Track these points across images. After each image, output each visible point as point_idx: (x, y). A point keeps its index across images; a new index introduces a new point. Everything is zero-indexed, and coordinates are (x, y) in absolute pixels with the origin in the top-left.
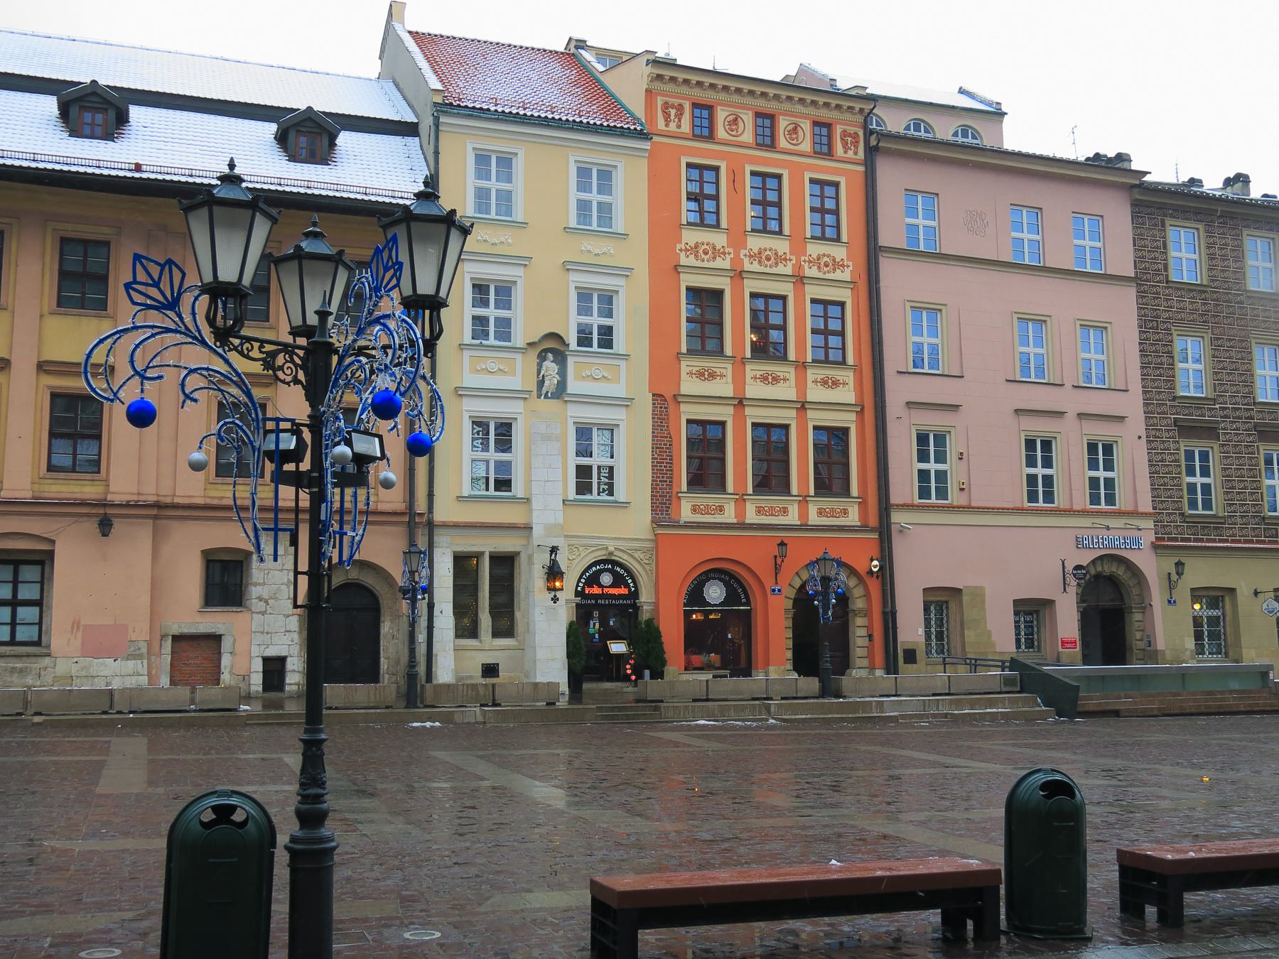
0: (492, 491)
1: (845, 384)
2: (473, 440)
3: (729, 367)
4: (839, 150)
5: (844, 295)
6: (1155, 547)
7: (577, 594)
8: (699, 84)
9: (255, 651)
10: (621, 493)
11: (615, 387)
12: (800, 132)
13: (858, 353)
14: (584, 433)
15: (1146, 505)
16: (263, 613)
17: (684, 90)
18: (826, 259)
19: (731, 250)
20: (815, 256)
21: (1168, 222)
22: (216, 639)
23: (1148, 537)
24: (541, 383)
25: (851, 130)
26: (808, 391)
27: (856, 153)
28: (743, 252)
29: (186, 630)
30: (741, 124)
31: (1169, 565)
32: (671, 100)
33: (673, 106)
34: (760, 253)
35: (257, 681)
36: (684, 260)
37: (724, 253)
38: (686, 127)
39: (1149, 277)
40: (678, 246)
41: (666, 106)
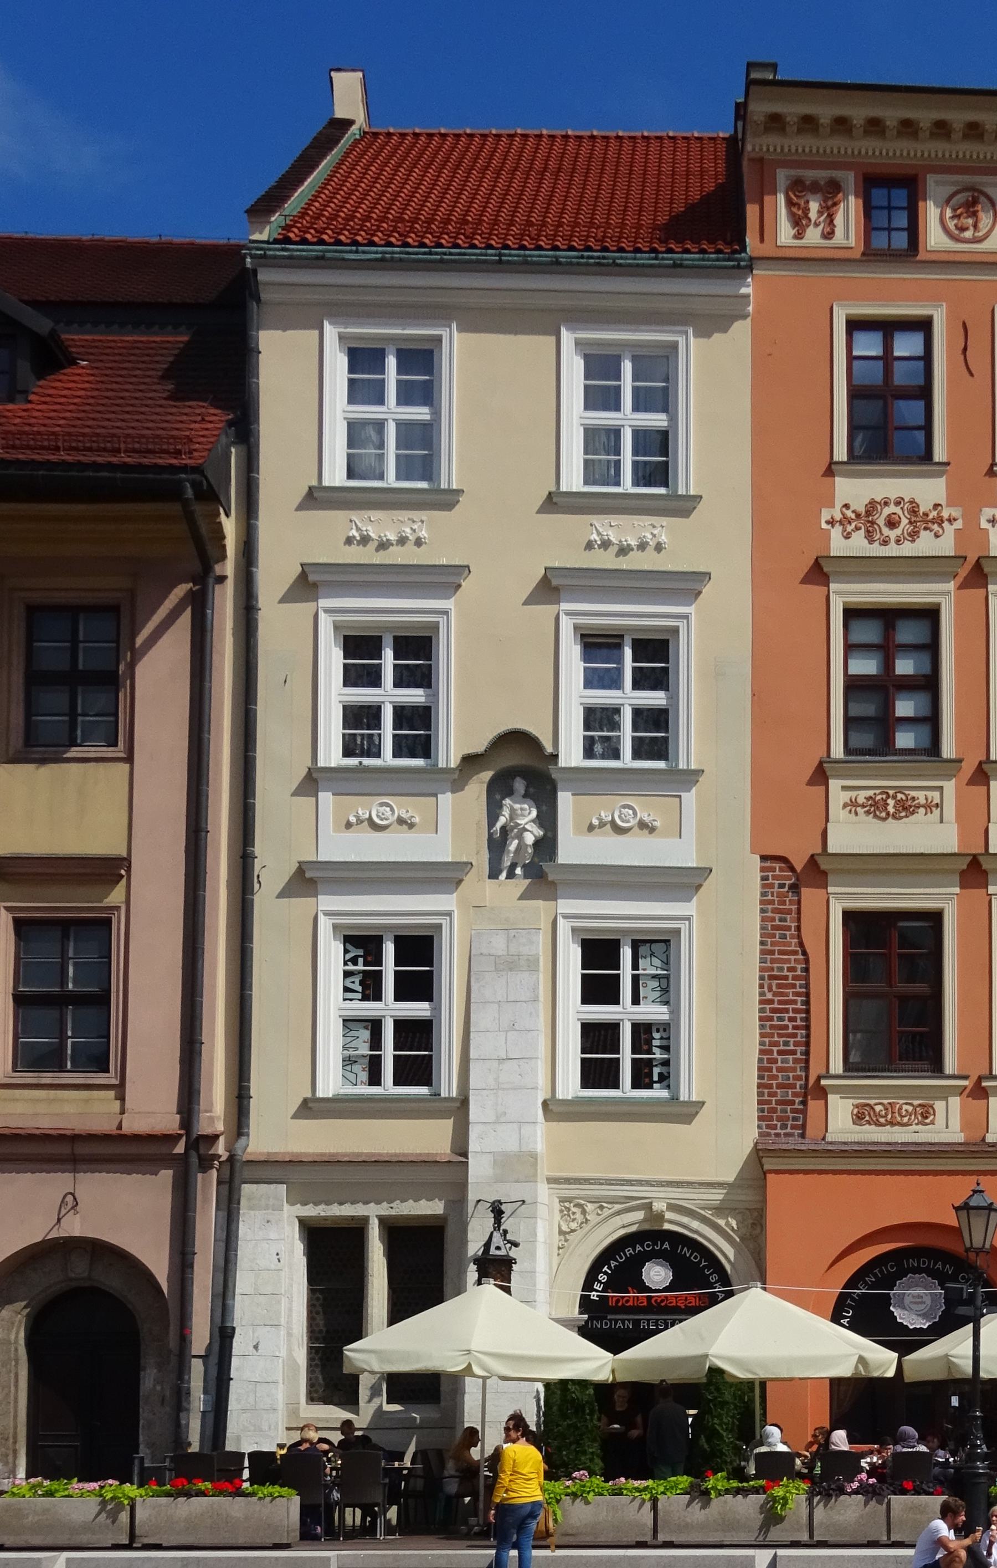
0: (388, 1086)
2: (347, 974)
7: (585, 1304)
10: (693, 1079)
11: (689, 841)
14: (599, 951)
19: (955, 512)
24: (497, 845)
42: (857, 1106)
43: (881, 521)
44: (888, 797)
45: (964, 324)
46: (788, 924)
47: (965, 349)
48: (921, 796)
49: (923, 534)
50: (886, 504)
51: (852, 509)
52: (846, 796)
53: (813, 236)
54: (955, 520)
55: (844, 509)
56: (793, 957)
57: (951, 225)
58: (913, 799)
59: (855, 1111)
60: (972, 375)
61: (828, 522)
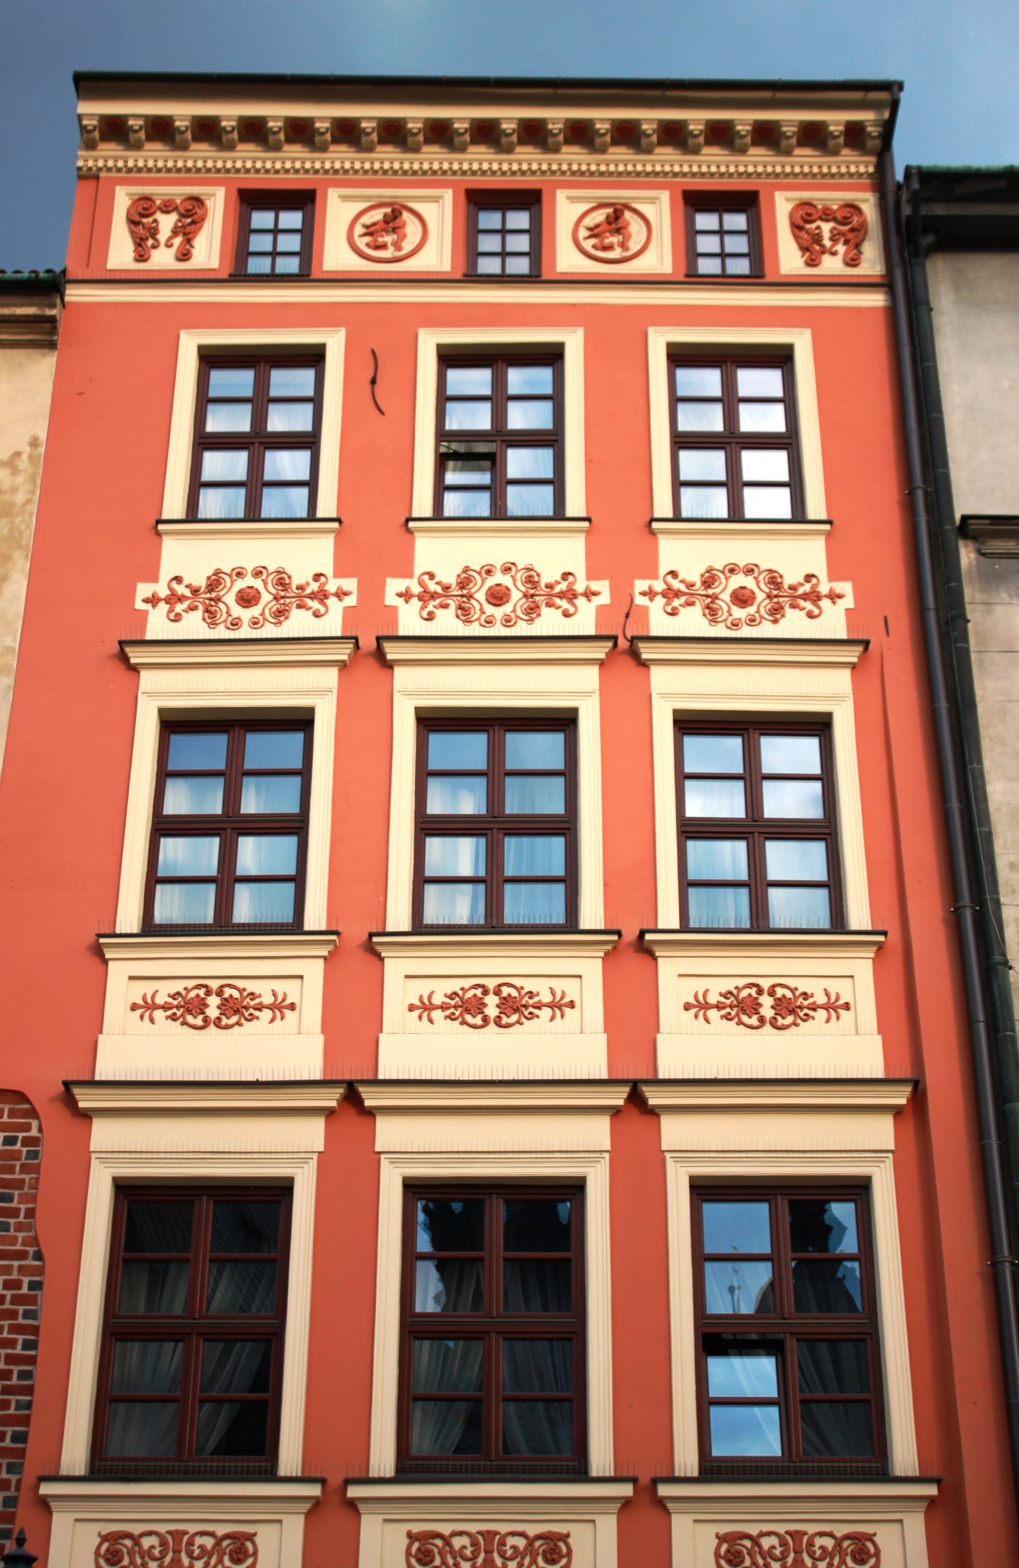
1: (834, 1007)
3: (314, 971)
4: (789, 258)
5: (826, 688)
12: (635, 228)
17: (202, 154)
18: (738, 581)
19: (350, 584)
20: (693, 574)
25: (833, 198)
26: (664, 1043)
27: (852, 262)
28: (394, 586)
30: (412, 229)
32: (161, 192)
33: (167, 208)
34: (464, 582)
37: (321, 596)
38: (209, 249)
40: (144, 590)
42: (104, 1538)
43: (230, 598)
44: (208, 993)
45: (373, 352)
46: (15, 1204)
47: (373, 382)
48: (265, 991)
49: (295, 613)
50: (239, 575)
51: (186, 582)
52: (138, 991)
53: (163, 259)
54: (346, 594)
55: (174, 584)
56: (16, 1264)
57: (362, 243)
58: (252, 995)
59: (105, 1546)
60: (382, 412)
61: (146, 601)
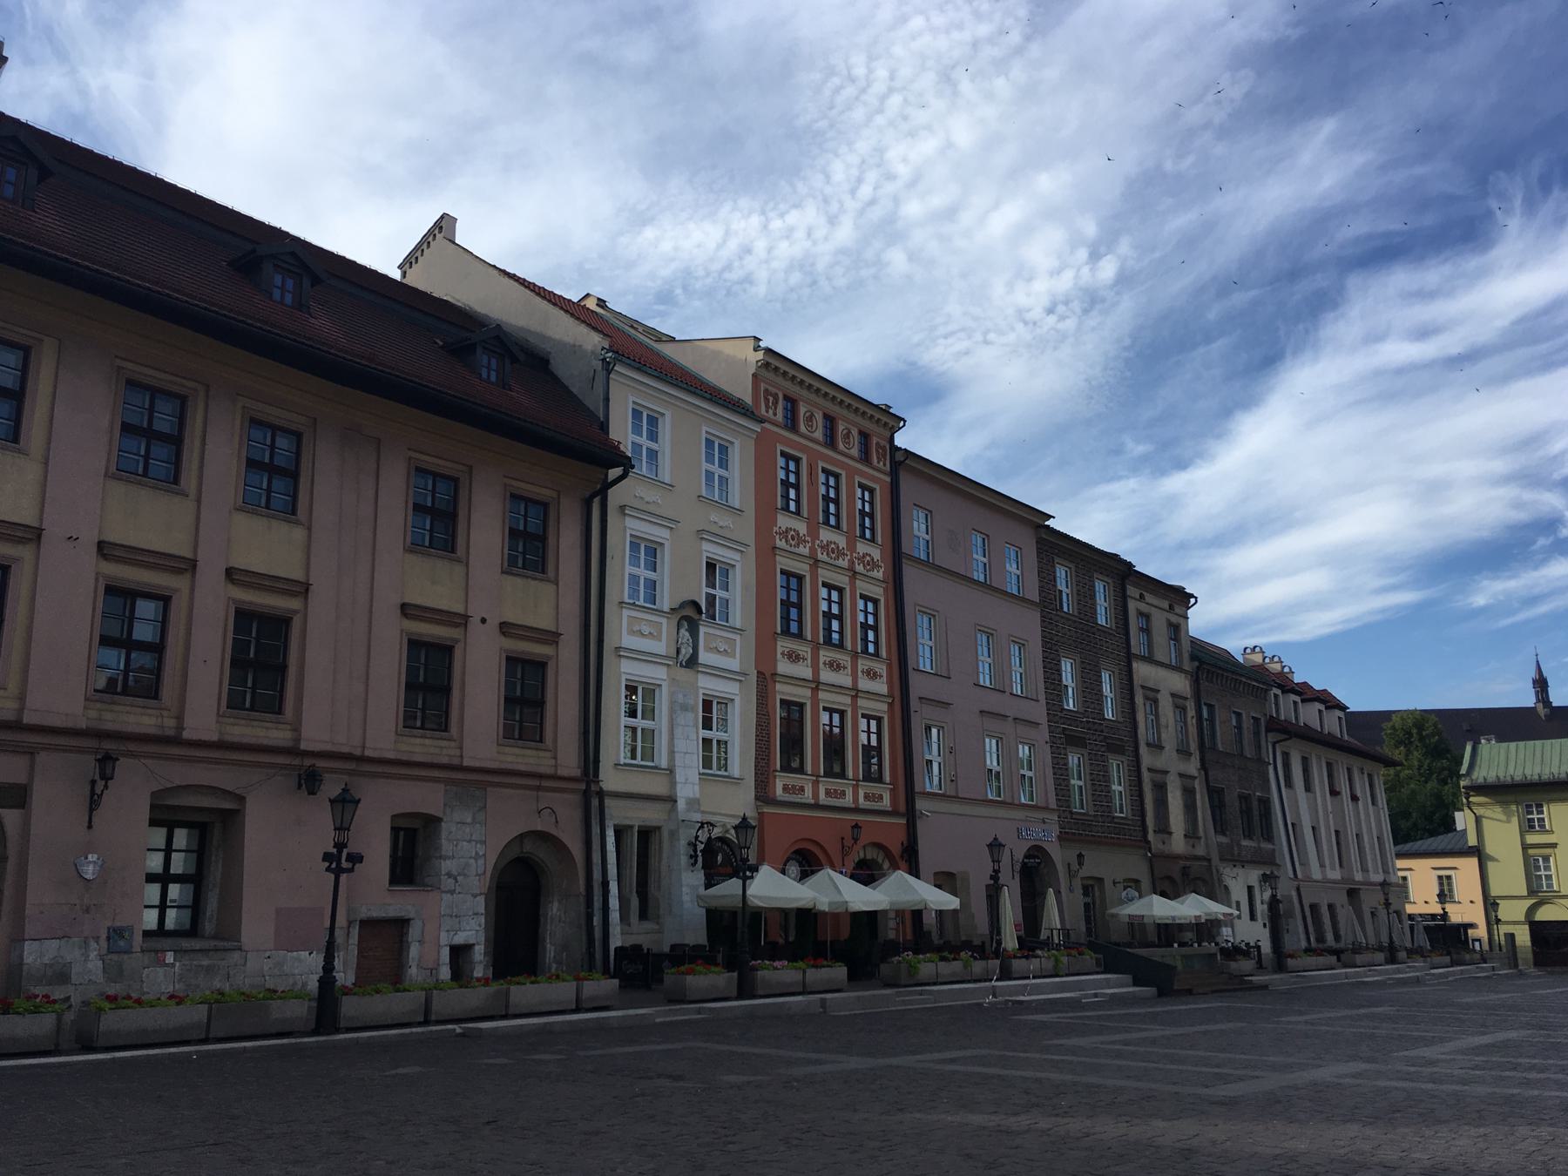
5: (877, 591)
6: (1060, 838)
8: (785, 373)
9: (444, 939)
13: (889, 652)
15: (1053, 804)
16: (452, 892)
21: (1057, 560)
22: (402, 924)
23: (1055, 831)
29: (376, 913)
31: (1071, 854)
35: (445, 973)
36: (781, 543)
39: (1048, 600)
41: (766, 391)
